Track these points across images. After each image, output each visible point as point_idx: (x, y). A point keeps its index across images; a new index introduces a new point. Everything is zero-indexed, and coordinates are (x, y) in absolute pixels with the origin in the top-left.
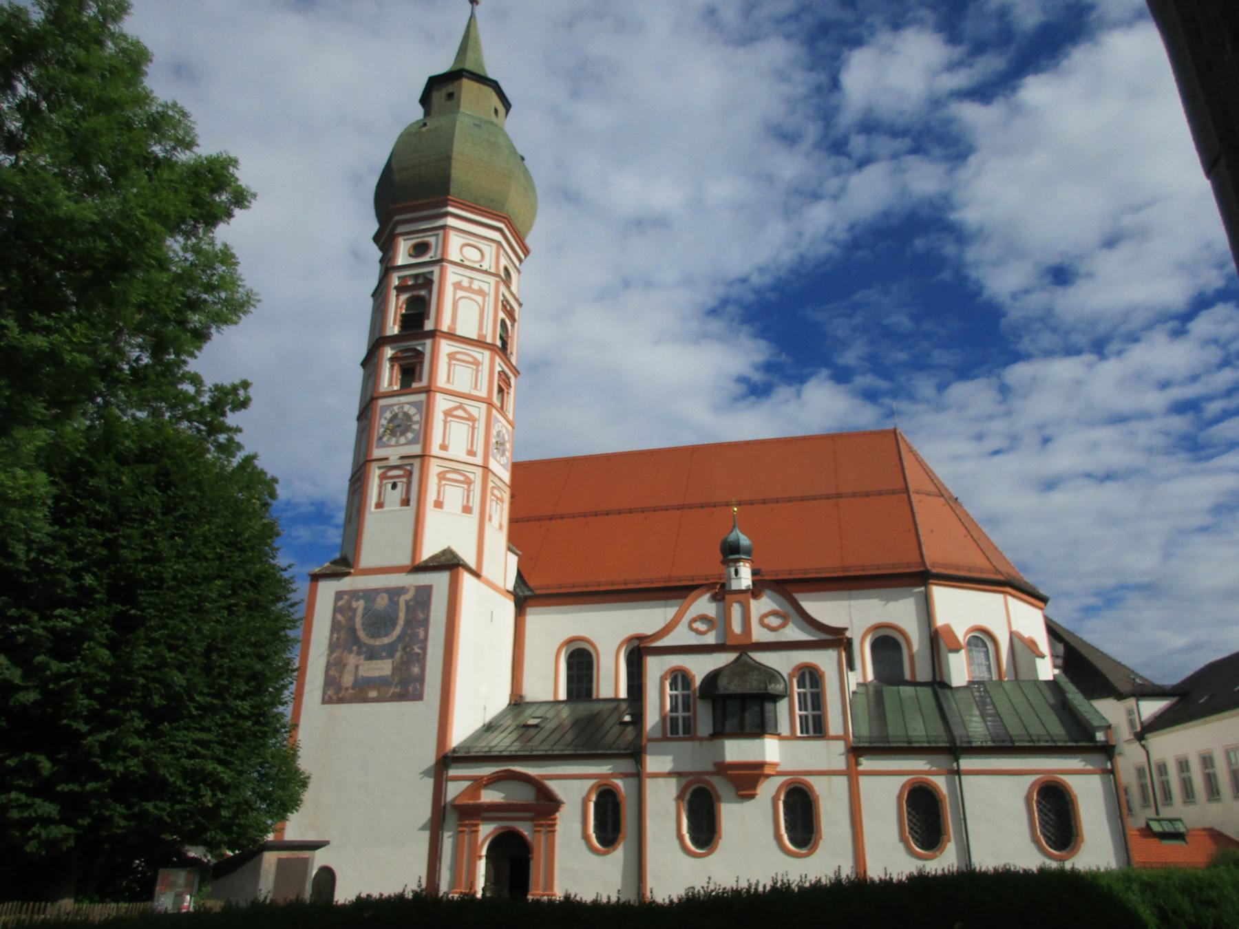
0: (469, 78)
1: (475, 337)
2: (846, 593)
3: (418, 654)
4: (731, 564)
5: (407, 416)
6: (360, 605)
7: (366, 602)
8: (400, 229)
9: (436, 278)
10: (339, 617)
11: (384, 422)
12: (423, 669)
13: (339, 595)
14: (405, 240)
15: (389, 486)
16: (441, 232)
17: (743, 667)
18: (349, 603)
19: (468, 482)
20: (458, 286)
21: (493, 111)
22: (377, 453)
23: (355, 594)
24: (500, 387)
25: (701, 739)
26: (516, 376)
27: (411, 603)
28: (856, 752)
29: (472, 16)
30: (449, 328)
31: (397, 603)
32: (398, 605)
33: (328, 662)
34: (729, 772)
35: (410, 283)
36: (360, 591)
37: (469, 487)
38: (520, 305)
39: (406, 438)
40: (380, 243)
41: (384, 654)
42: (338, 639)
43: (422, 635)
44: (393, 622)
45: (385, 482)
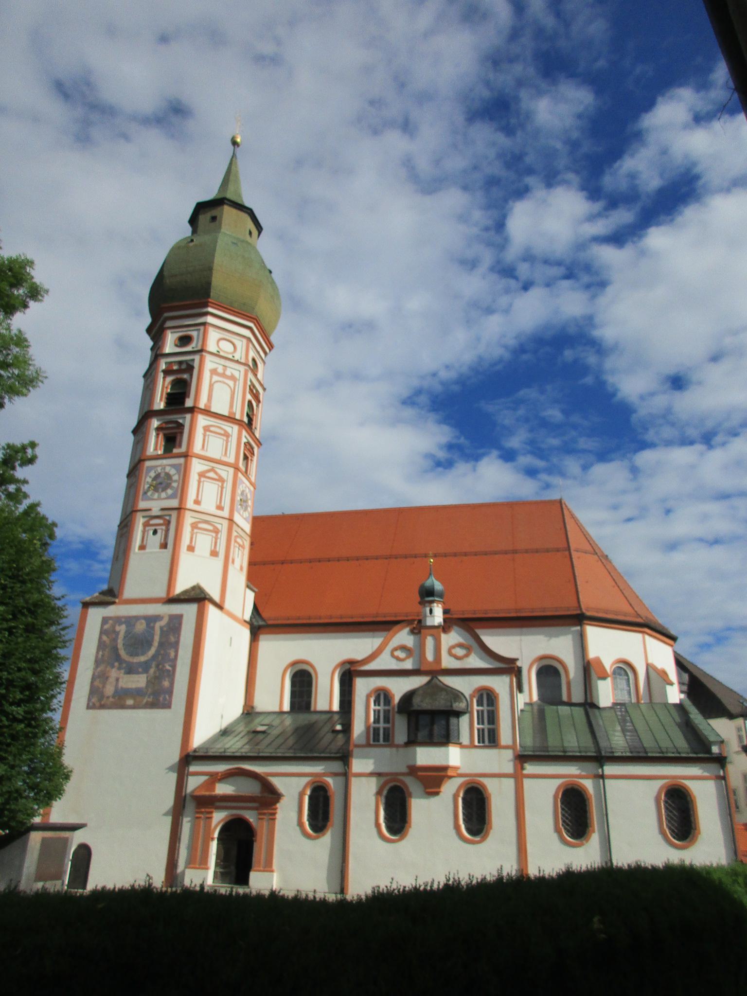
0: (230, 206)
1: (226, 414)
2: (518, 630)
3: (168, 671)
4: (427, 605)
5: (168, 476)
6: (122, 629)
8: (169, 324)
9: (196, 364)
10: (105, 638)
11: (149, 480)
12: (172, 683)
13: (105, 620)
14: (172, 333)
15: (151, 532)
16: (202, 328)
17: (433, 688)
18: (113, 626)
19: (216, 531)
20: (214, 372)
21: (248, 232)
22: (142, 505)
23: (118, 620)
24: (245, 455)
25: (398, 746)
26: (258, 447)
27: (165, 629)
28: (522, 759)
29: (234, 155)
30: (205, 406)
31: (153, 628)
32: (154, 630)
33: (94, 675)
34: (420, 773)
35: (175, 367)
36: (123, 617)
37: (217, 535)
38: (264, 389)
39: (167, 494)
40: (152, 335)
42: (103, 656)
43: (172, 654)
44: (150, 644)
45: (147, 528)
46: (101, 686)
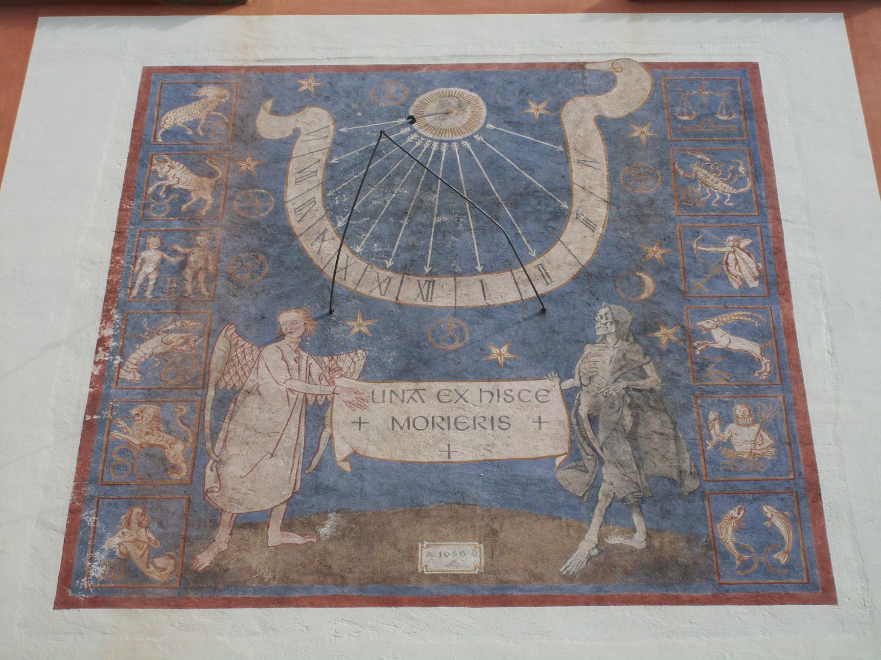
7: (339, 119)
27: (641, 132)
41: (500, 353)
46: (177, 452)
